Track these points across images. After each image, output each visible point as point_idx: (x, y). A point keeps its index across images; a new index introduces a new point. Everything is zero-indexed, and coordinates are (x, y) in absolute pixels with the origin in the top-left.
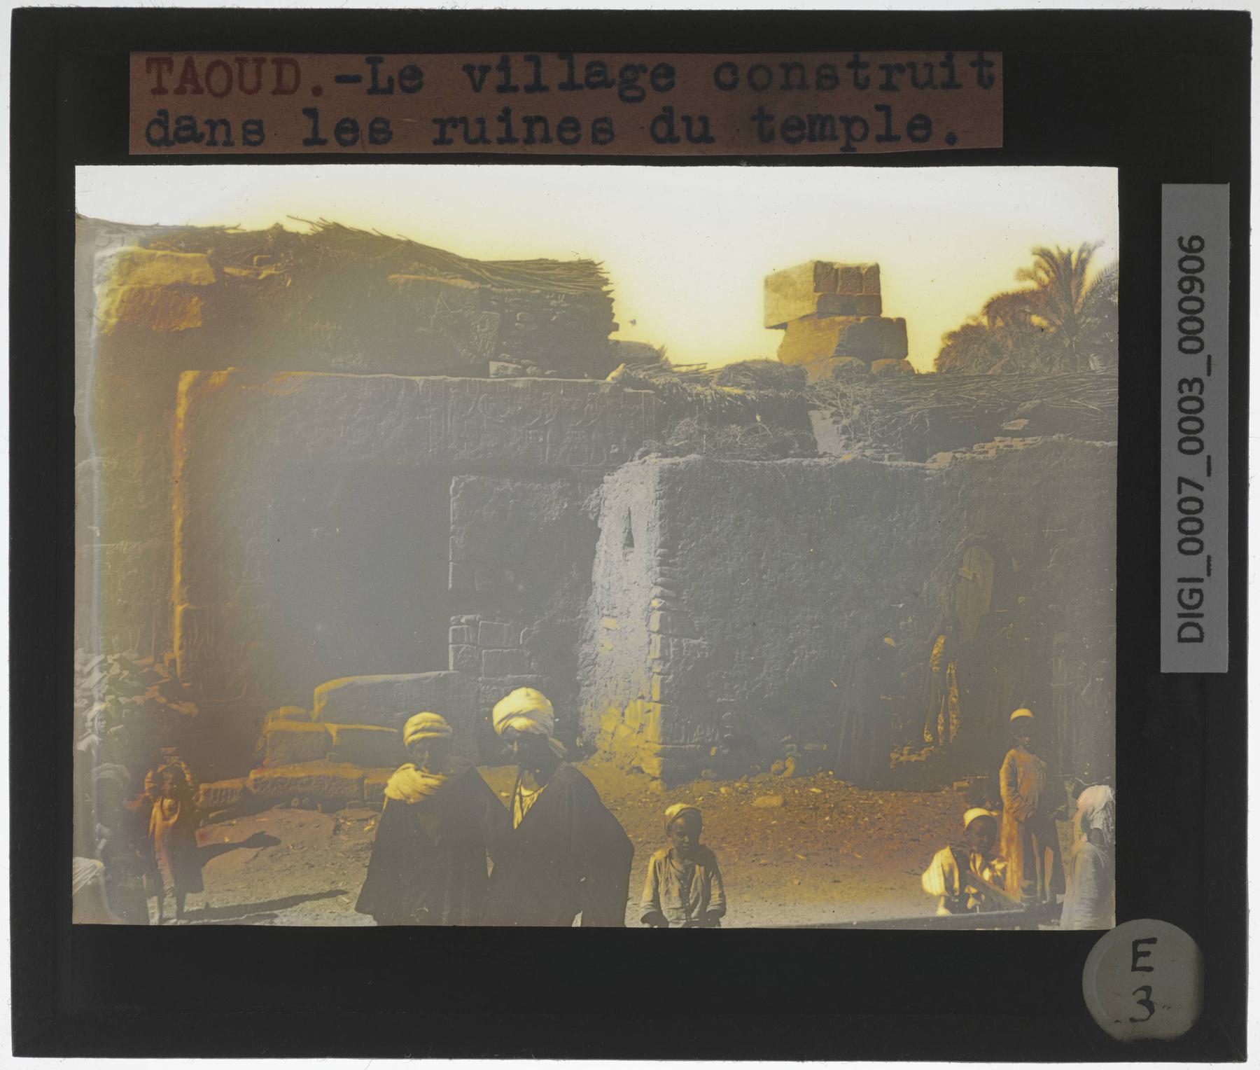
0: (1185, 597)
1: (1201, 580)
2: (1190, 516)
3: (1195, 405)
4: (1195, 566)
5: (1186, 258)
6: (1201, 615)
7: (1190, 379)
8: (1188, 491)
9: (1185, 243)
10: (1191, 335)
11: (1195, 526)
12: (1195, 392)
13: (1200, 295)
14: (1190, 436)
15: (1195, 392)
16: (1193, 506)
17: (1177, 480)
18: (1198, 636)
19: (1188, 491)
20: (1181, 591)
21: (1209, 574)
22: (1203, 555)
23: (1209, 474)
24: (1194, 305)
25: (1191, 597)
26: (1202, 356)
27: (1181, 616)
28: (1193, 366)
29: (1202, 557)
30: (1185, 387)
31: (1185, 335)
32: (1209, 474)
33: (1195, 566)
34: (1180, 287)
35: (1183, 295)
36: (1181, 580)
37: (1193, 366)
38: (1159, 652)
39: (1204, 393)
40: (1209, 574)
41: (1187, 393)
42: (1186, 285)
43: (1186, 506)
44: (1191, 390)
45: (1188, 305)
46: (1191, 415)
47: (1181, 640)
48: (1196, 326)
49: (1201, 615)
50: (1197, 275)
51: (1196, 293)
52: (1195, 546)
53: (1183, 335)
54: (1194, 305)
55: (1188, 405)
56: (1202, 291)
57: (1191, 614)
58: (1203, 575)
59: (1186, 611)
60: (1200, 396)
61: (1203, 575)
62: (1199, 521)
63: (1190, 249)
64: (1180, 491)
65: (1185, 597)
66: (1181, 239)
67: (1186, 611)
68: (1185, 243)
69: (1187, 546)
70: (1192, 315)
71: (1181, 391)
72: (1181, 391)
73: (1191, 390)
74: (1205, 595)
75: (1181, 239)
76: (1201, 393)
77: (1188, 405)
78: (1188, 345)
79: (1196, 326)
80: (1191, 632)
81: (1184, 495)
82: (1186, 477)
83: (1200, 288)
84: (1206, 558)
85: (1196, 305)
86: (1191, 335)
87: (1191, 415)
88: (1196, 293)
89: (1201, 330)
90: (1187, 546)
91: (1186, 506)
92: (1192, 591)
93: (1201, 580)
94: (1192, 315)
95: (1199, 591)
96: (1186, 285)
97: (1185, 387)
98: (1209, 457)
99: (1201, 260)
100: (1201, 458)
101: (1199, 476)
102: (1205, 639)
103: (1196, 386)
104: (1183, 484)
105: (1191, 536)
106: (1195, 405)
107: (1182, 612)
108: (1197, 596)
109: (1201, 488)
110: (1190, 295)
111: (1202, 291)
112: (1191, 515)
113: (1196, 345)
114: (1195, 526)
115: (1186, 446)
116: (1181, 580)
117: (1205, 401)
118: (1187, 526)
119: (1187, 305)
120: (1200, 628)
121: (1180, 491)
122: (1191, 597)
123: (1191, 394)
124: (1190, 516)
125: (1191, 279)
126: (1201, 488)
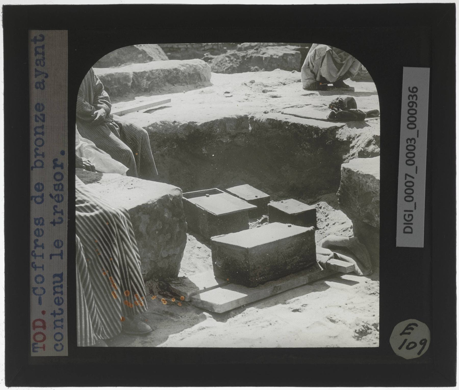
0: (407, 217)
1: (412, 211)
2: (409, 188)
3: (412, 148)
4: (410, 206)
5: (409, 153)
6: (412, 224)
7: (411, 138)
8: (409, 179)
9: (411, 89)
10: (412, 123)
11: (411, 191)
12: (412, 143)
14: (410, 159)
19: (409, 179)
20: (405, 215)
21: (415, 209)
23: (416, 173)
24: (414, 112)
25: (409, 217)
26: (415, 130)
27: (405, 224)
28: (412, 134)
29: (412, 204)
30: (409, 141)
31: (409, 122)
32: (416, 173)
33: (410, 206)
36: (405, 211)
37: (412, 134)
38: (398, 168)
40: (415, 209)
41: (409, 143)
42: (411, 104)
43: (408, 184)
44: (411, 142)
45: (411, 112)
46: (410, 151)
47: (405, 232)
48: (414, 119)
49: (412, 224)
51: (414, 107)
52: (411, 199)
54: (413, 112)
55: (410, 148)
56: (416, 107)
57: (408, 223)
58: (413, 209)
59: (407, 222)
60: (414, 145)
61: (413, 209)
64: (406, 179)
65: (407, 217)
66: (409, 88)
67: (407, 222)
68: (411, 89)
69: (407, 199)
70: (412, 115)
71: (407, 143)
72: (407, 143)
73: (411, 142)
74: (413, 216)
75: (409, 88)
76: (414, 143)
77: (410, 148)
78: (410, 126)
79: (414, 119)
80: (408, 230)
81: (407, 180)
82: (409, 174)
84: (414, 204)
85: (414, 112)
86: (412, 123)
87: (410, 151)
88: (414, 107)
89: (415, 121)
90: (407, 199)
91: (408, 184)
92: (409, 215)
93: (412, 211)
94: (412, 115)
95: (412, 215)
96: (411, 104)
97: (409, 141)
98: (417, 167)
99: (414, 154)
101: (413, 174)
103: (413, 141)
104: (407, 176)
105: (409, 195)
106: (412, 148)
107: (405, 222)
108: (411, 217)
109: (413, 178)
110: (412, 108)
111: (416, 107)
112: (410, 187)
113: (413, 126)
114: (411, 191)
116: (405, 211)
118: (408, 191)
119: (411, 112)
121: (406, 179)
122: (409, 217)
124: (409, 188)
125: (412, 105)
126: (413, 178)
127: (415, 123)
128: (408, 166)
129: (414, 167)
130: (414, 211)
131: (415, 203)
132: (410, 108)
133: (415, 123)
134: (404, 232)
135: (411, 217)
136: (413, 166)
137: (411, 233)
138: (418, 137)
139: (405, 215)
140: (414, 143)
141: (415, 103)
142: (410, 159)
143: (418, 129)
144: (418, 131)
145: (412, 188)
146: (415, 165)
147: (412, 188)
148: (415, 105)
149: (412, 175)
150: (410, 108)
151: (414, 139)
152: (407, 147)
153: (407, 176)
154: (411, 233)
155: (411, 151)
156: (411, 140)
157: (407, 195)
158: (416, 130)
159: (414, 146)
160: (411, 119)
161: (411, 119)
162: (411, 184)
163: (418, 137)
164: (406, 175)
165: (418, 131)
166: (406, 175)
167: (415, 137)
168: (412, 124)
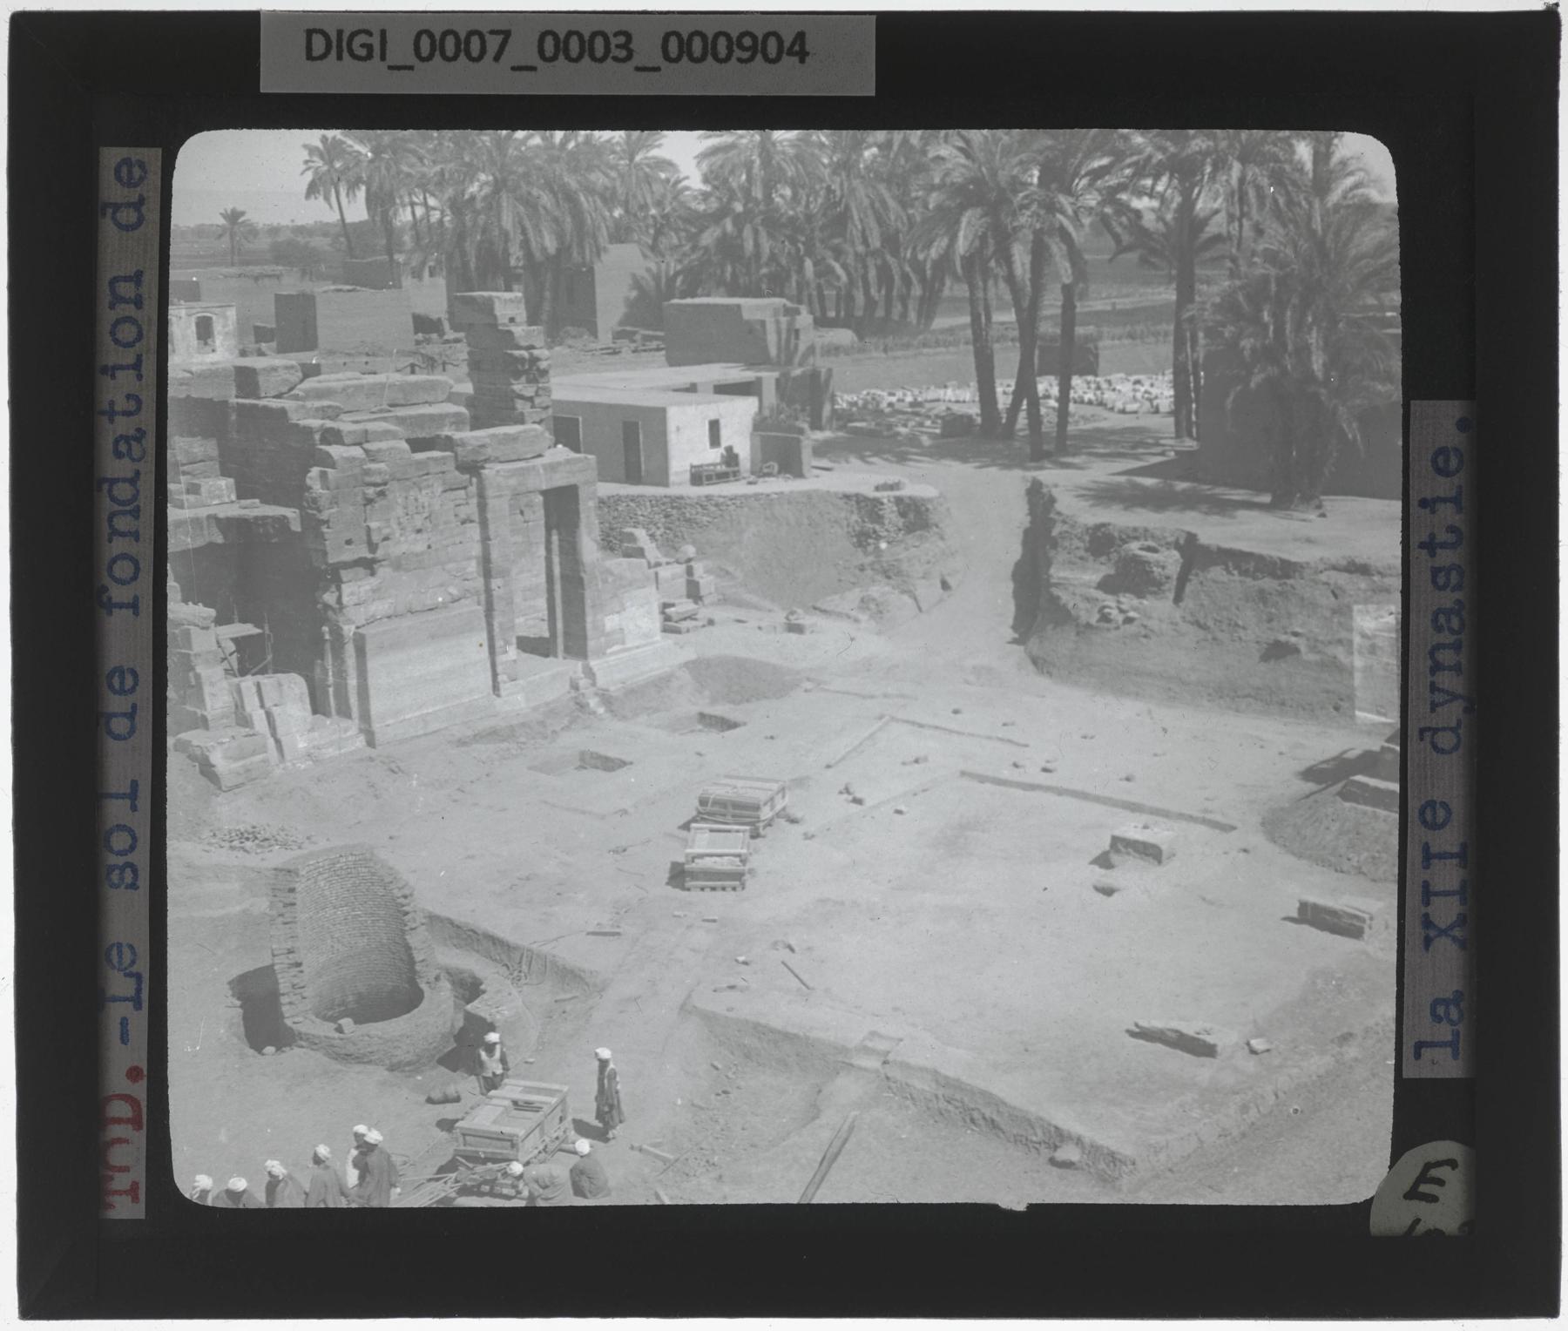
1: (383, 58)
3: (599, 51)
6: (340, 58)
7: (631, 46)
8: (493, 43)
10: (685, 47)
13: (734, 59)
15: (616, 52)
16: (475, 52)
17: (503, 28)
18: (316, 53)
19: (493, 43)
20: (369, 33)
21: (390, 68)
22: (413, 60)
23: (513, 69)
25: (363, 46)
26: (658, 59)
29: (412, 60)
30: (622, 39)
32: (513, 69)
33: (400, 51)
35: (734, 35)
39: (615, 64)
40: (390, 68)
41: (614, 41)
43: (475, 41)
44: (617, 46)
45: (722, 42)
47: (310, 33)
49: (340, 58)
50: (759, 56)
51: (738, 53)
53: (685, 37)
55: (599, 44)
56: (740, 60)
58: (392, 59)
60: (609, 60)
61: (392, 59)
62: (455, 58)
63: (753, 49)
64: (492, 32)
71: (616, 34)
72: (616, 34)
76: (616, 59)
81: (488, 37)
82: (510, 40)
84: (408, 63)
86: (685, 47)
87: (587, 47)
88: (738, 53)
90: (425, 43)
91: (475, 41)
92: (369, 47)
93: (383, 58)
95: (369, 56)
96: (747, 42)
97: (622, 39)
101: (510, 57)
102: (309, 62)
103: (623, 53)
104: (500, 38)
106: (599, 51)
108: (363, 52)
109: (497, 58)
111: (740, 60)
115: (549, 44)
116: (383, 33)
117: (604, 65)
119: (722, 42)
120: (323, 57)
121: (492, 32)
122: (363, 46)
123: (613, 46)
126: (497, 58)
127: (710, 58)
129: (535, 60)
130: (383, 66)
131: (411, 68)
132: (734, 39)
133: (685, 58)
135: (363, 52)
137: (310, 57)
138: (638, 69)
139: (369, 33)
141: (751, 59)
143: (662, 68)
144: (657, 69)
146: (542, 62)
148: (746, 55)
150: (734, 39)
151: (629, 57)
153: (500, 38)
154: (310, 57)
156: (625, 46)
157: (438, 37)
159: (602, 60)
162: (475, 52)
163: (638, 69)
164: (507, 34)
165: (657, 69)
166: (507, 34)
167: (637, 60)
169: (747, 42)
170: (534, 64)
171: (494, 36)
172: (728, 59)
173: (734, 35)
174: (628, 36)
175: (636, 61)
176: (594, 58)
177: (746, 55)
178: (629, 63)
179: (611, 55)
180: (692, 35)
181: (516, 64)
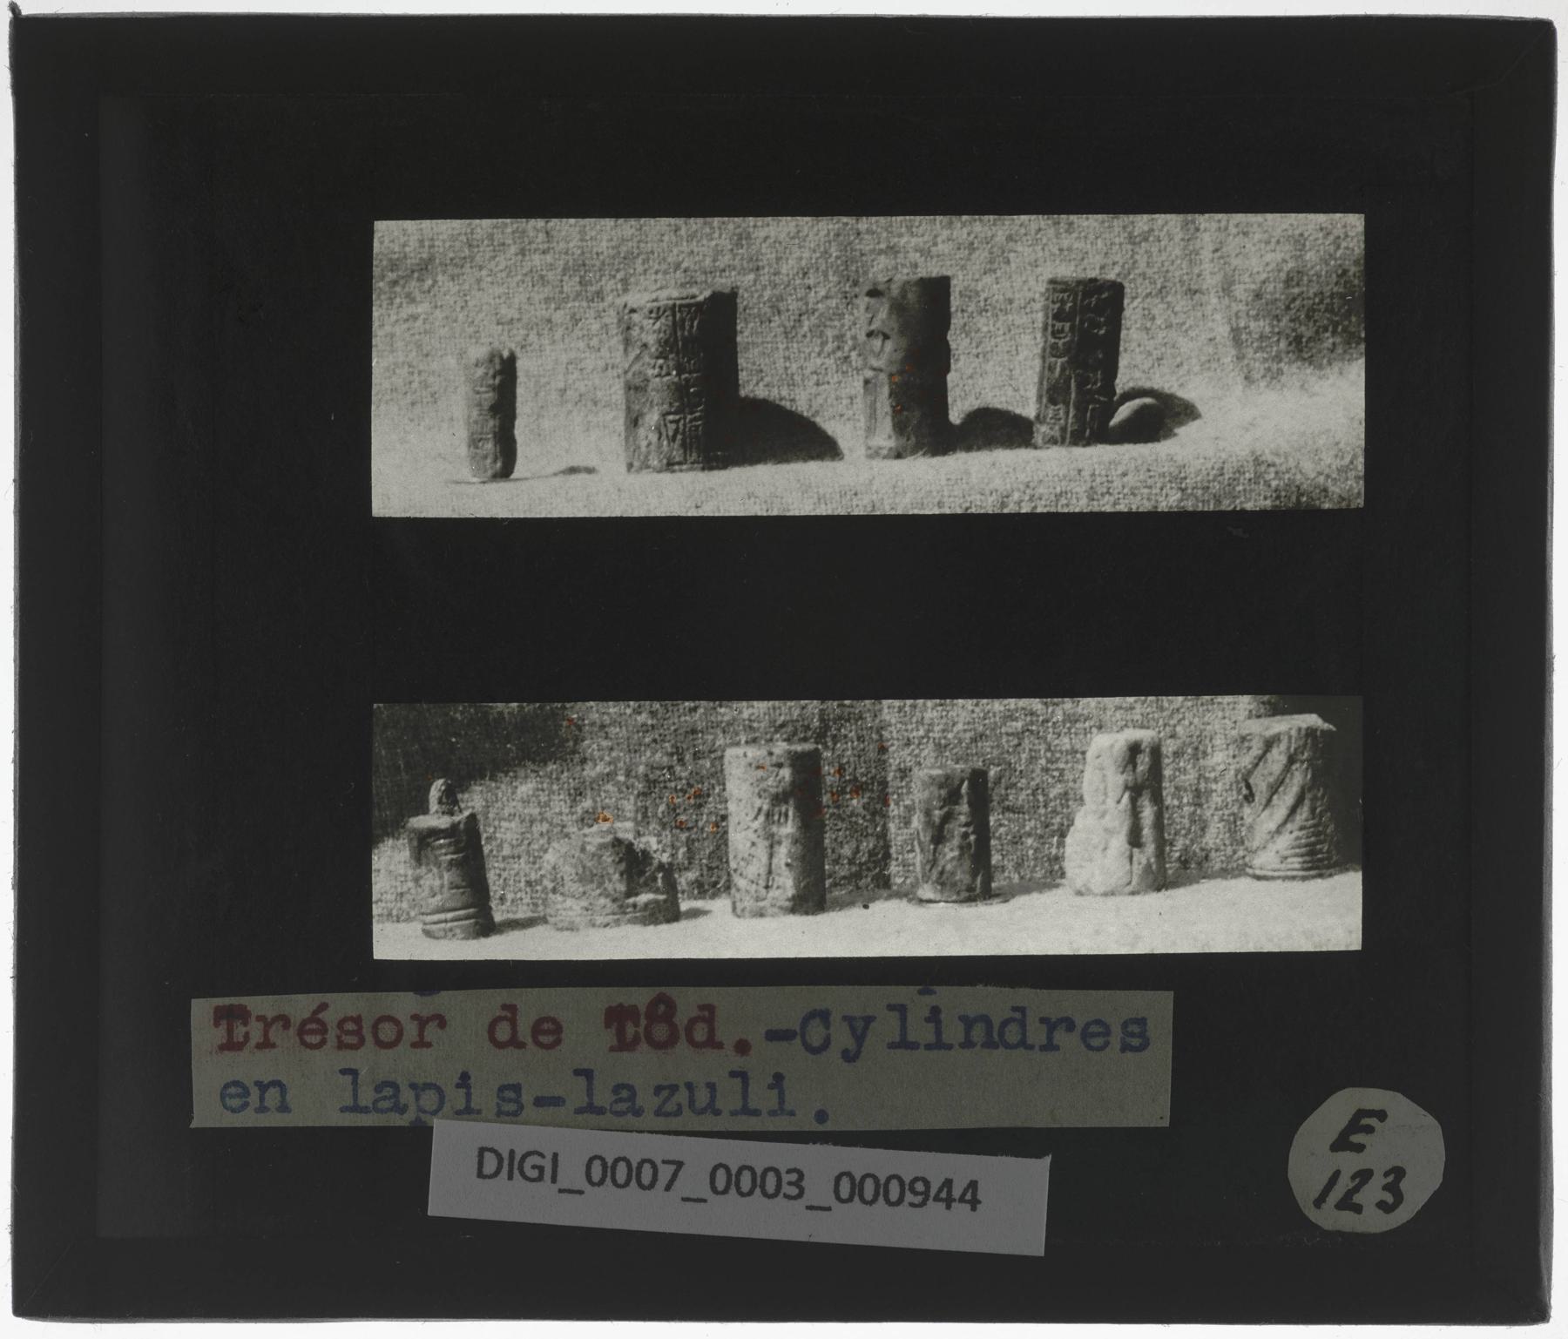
7: (804, 1184)
10: (857, 1188)
12: (787, 1189)
13: (906, 1203)
14: (733, 1180)
15: (787, 1189)
17: (681, 1160)
23: (685, 1200)
24: (894, 1196)
26: (831, 1200)
28: (819, 1189)
30: (794, 1177)
32: (685, 1200)
34: (916, 1179)
35: (907, 1180)
37: (819, 1189)
41: (786, 1178)
42: (920, 1187)
44: (790, 1183)
45: (894, 1185)
46: (758, 1182)
51: (909, 1197)
54: (894, 1194)
55: (771, 1181)
56: (912, 1205)
60: (781, 1195)
70: (882, 1189)
71: (789, 1172)
72: (789, 1172)
73: (790, 1183)
76: (786, 1196)
77: (771, 1181)
83: (916, 1202)
85: (894, 1196)
87: (758, 1182)
88: (909, 1197)
94: (882, 1189)
97: (794, 1177)
100: (705, 1192)
101: (684, 1186)
103: (794, 1191)
111: (912, 1205)
115: (721, 1177)
125: (920, 1192)
128: (710, 1170)
133: (856, 1198)
134: (482, 1151)
136: (708, 1187)
140: (786, 1196)
141: (923, 1204)
142: (733, 1180)
144: (829, 1209)
145: (634, 1182)
147: (633, 1182)
148: (918, 1200)
149: (677, 1184)
152: (777, 1172)
153: (673, 1168)
155: (760, 1183)
156: (797, 1184)
158: (832, 1201)
160: (869, 1186)
161: (869, 1186)
163: (810, 1208)
166: (680, 1165)
167: (811, 1197)
168: (854, 1189)
169: (920, 1187)
170: (704, 1197)
171: (666, 1166)
172: (900, 1201)
173: (907, 1180)
174: (801, 1175)
175: (810, 1198)
176: (765, 1194)
177: (918, 1200)
178: (799, 1200)
179: (783, 1191)
180: (864, 1177)
181: (685, 1196)
